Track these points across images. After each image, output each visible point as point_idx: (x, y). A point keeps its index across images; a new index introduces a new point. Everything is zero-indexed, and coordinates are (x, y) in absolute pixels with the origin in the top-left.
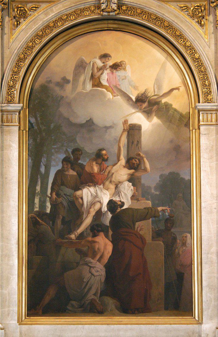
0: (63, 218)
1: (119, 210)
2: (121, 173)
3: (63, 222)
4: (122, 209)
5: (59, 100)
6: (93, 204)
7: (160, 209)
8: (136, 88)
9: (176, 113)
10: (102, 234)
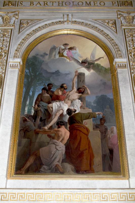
0: (41, 118)
1: (73, 114)
2: (74, 95)
3: (41, 120)
4: (75, 113)
5: (41, 63)
6: (58, 111)
7: (97, 113)
8: (81, 57)
9: (103, 68)
10: (63, 127)
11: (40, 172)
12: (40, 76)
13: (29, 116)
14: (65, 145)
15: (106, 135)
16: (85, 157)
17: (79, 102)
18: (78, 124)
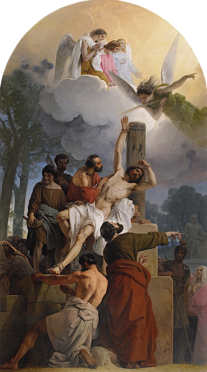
0: (45, 246)
1: (116, 235)
2: (119, 187)
3: (45, 251)
4: (120, 234)
5: (37, 91)
6: (82, 228)
7: (169, 234)
8: (138, 75)
9: (189, 108)
10: (94, 267)
11: (49, 365)
12: (37, 135)
13: (16, 241)
14: (98, 308)
15: (186, 285)
16: (138, 335)
17: (130, 205)
18: (127, 262)
